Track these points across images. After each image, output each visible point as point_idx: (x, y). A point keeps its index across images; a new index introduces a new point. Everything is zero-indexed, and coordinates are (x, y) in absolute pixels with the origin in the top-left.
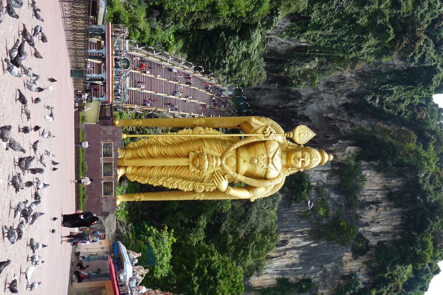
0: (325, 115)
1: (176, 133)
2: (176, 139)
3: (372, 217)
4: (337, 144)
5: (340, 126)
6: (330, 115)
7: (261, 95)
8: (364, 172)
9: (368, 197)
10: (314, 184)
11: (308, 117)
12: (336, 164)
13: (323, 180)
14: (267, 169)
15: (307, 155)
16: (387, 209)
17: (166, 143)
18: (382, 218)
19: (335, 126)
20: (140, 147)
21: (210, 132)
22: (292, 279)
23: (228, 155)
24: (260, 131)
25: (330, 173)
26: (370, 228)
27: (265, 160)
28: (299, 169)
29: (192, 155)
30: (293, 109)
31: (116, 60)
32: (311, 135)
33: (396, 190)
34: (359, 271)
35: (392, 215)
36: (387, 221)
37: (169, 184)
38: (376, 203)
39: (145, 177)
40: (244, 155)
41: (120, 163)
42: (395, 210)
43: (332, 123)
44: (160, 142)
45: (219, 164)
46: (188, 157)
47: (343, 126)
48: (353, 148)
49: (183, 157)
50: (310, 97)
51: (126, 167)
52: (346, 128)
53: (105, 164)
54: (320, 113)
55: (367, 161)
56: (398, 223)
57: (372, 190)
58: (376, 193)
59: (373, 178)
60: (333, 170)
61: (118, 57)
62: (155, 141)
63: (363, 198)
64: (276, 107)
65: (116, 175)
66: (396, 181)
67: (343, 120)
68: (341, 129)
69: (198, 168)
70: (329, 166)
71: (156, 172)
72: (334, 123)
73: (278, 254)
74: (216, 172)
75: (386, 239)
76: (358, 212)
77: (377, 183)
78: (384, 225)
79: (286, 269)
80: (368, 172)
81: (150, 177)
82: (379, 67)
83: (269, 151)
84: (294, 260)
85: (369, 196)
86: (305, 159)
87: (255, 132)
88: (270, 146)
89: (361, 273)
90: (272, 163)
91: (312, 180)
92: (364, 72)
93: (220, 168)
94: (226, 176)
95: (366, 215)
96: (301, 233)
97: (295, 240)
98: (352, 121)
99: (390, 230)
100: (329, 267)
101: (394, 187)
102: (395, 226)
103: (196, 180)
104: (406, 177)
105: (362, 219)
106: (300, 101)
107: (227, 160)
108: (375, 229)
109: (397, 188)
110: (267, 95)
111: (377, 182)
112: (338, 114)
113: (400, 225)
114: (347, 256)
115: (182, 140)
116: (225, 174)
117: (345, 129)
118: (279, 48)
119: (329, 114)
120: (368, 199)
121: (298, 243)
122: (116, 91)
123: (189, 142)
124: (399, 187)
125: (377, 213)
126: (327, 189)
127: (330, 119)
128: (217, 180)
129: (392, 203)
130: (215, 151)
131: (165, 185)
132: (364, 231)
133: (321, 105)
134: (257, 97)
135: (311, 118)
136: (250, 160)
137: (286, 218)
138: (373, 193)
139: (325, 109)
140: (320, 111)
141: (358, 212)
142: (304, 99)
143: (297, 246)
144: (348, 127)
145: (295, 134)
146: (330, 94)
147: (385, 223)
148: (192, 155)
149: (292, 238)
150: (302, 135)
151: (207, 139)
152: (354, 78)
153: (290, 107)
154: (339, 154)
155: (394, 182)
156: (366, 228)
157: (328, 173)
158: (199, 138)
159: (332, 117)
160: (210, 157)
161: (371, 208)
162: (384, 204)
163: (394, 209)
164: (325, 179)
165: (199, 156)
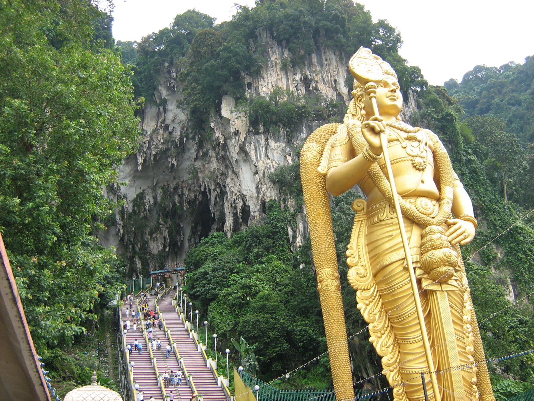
0: (140, 168)
1: (370, 327)
2: (382, 323)
3: (328, 89)
4: (216, 131)
5: (156, 148)
6: (140, 161)
8: (262, 94)
9: (300, 91)
10: (289, 159)
11: (137, 195)
12: (254, 128)
13: (281, 147)
14: (426, 144)
16: (314, 70)
17: (394, 346)
18: (328, 77)
19: (155, 156)
21: (356, 255)
24: (375, 140)
25: (269, 138)
26: (343, 93)
29: (425, 284)
30: (125, 215)
33: (286, 54)
35: (321, 65)
36: (331, 71)
37: (467, 339)
38: (306, 81)
43: (150, 159)
44: (394, 359)
47: (157, 144)
48: (223, 106)
49: (427, 305)
52: (160, 141)
54: (134, 177)
55: (245, 91)
56: (333, 56)
57: (288, 86)
58: (293, 80)
59: (270, 84)
60: (264, 133)
62: (395, 371)
64: (122, 240)
66: (272, 56)
67: (148, 143)
68: (161, 147)
70: (259, 138)
72: (151, 156)
74: (450, 238)
76: (323, 104)
77: (277, 80)
78: (337, 74)
80: (261, 89)
90: (414, 133)
91: (282, 164)
94: (451, 221)
95: (327, 96)
98: (149, 133)
99: (343, 68)
101: (282, 58)
102: (337, 62)
104: (267, 43)
109: (283, 54)
111: (275, 79)
115: (381, 312)
116: (446, 222)
117: (162, 141)
119: (138, 162)
120: (301, 92)
125: (321, 81)
126: (295, 143)
127: (145, 161)
128: (462, 237)
133: (122, 174)
135: (139, 191)
136: (417, 171)
138: (292, 85)
140: (130, 176)
141: (323, 104)
142: (112, 197)
144: (159, 138)
145: (370, 78)
147: (336, 72)
153: (123, 218)
154: (232, 129)
155: (275, 57)
157: (269, 140)
158: (375, 276)
159: (143, 158)
161: (316, 89)
162: (308, 73)
163: (313, 61)
164: (278, 144)
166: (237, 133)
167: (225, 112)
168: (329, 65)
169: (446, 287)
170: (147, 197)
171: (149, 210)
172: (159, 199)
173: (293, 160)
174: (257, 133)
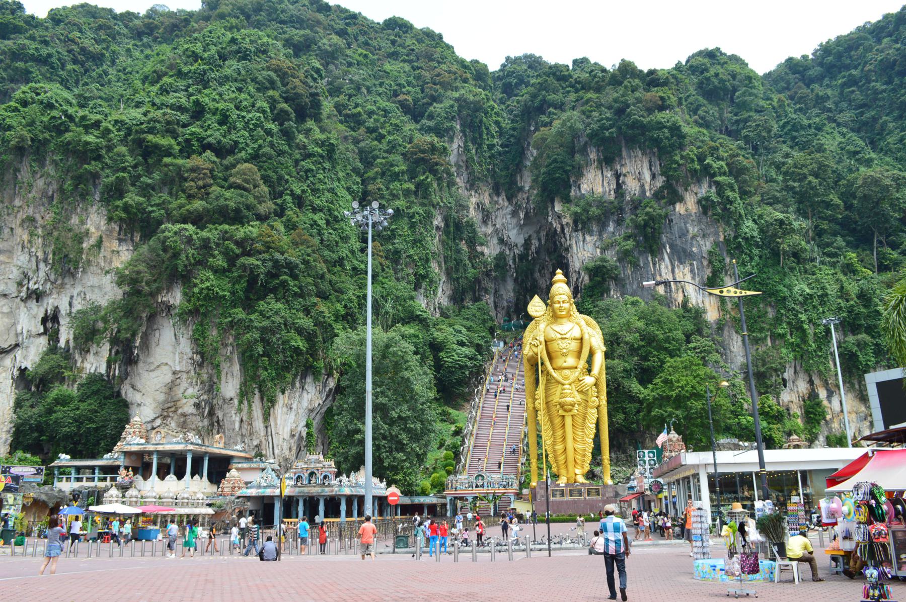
0: (522, 222)
6: (522, 216)
7: (503, 299)
8: (583, 192)
10: (598, 250)
15: (557, 298)
19: (534, 209)
20: (556, 461)
22: (708, 272)
23: (560, 379)
24: (535, 350)
27: (564, 341)
28: (571, 305)
31: (477, 486)
32: (536, 299)
34: (696, 194)
35: (630, 157)
38: (617, 176)
39: (584, 456)
40: (560, 362)
41: (572, 481)
42: (624, 153)
45: (568, 387)
46: (563, 416)
48: (556, 203)
50: (501, 241)
51: (576, 474)
53: (571, 496)
55: (570, 187)
60: (582, 229)
61: (474, 485)
63: (612, 192)
64: (516, 280)
65: (582, 484)
69: (573, 406)
71: (579, 447)
73: (680, 290)
75: (658, 163)
79: (697, 279)
81: (585, 450)
82: (461, 163)
83: (554, 337)
84: (687, 270)
85: (609, 185)
86: (561, 300)
87: (537, 354)
88: (550, 337)
89: (699, 190)
92: (468, 181)
93: (573, 385)
96: (654, 264)
97: (663, 271)
100: (693, 230)
103: (586, 407)
105: (637, 193)
106: (507, 252)
107: (566, 378)
108: (647, 176)
110: (503, 292)
112: (520, 206)
113: (641, 149)
114: (679, 208)
118: (448, 292)
121: (667, 267)
122: (505, 487)
123: (549, 415)
124: (598, 150)
127: (526, 214)
129: (617, 159)
130: (557, 391)
131: (592, 436)
132: (651, 189)
134: (505, 304)
135: (527, 236)
137: (638, 283)
139: (514, 221)
141: (628, 198)
143: (670, 268)
146: (496, 217)
148: (561, 412)
149: (661, 275)
150: (537, 309)
151: (546, 397)
152: (476, 192)
155: (593, 156)
156: (647, 187)
160: (563, 396)
161: (623, 182)
162: (618, 167)
165: (562, 406)
166: (567, 224)
167: (558, 207)
168: (635, 157)
169: (570, 413)
170: (533, 242)
171: (536, 252)
172: (543, 242)
173: (601, 253)
174: (576, 230)
